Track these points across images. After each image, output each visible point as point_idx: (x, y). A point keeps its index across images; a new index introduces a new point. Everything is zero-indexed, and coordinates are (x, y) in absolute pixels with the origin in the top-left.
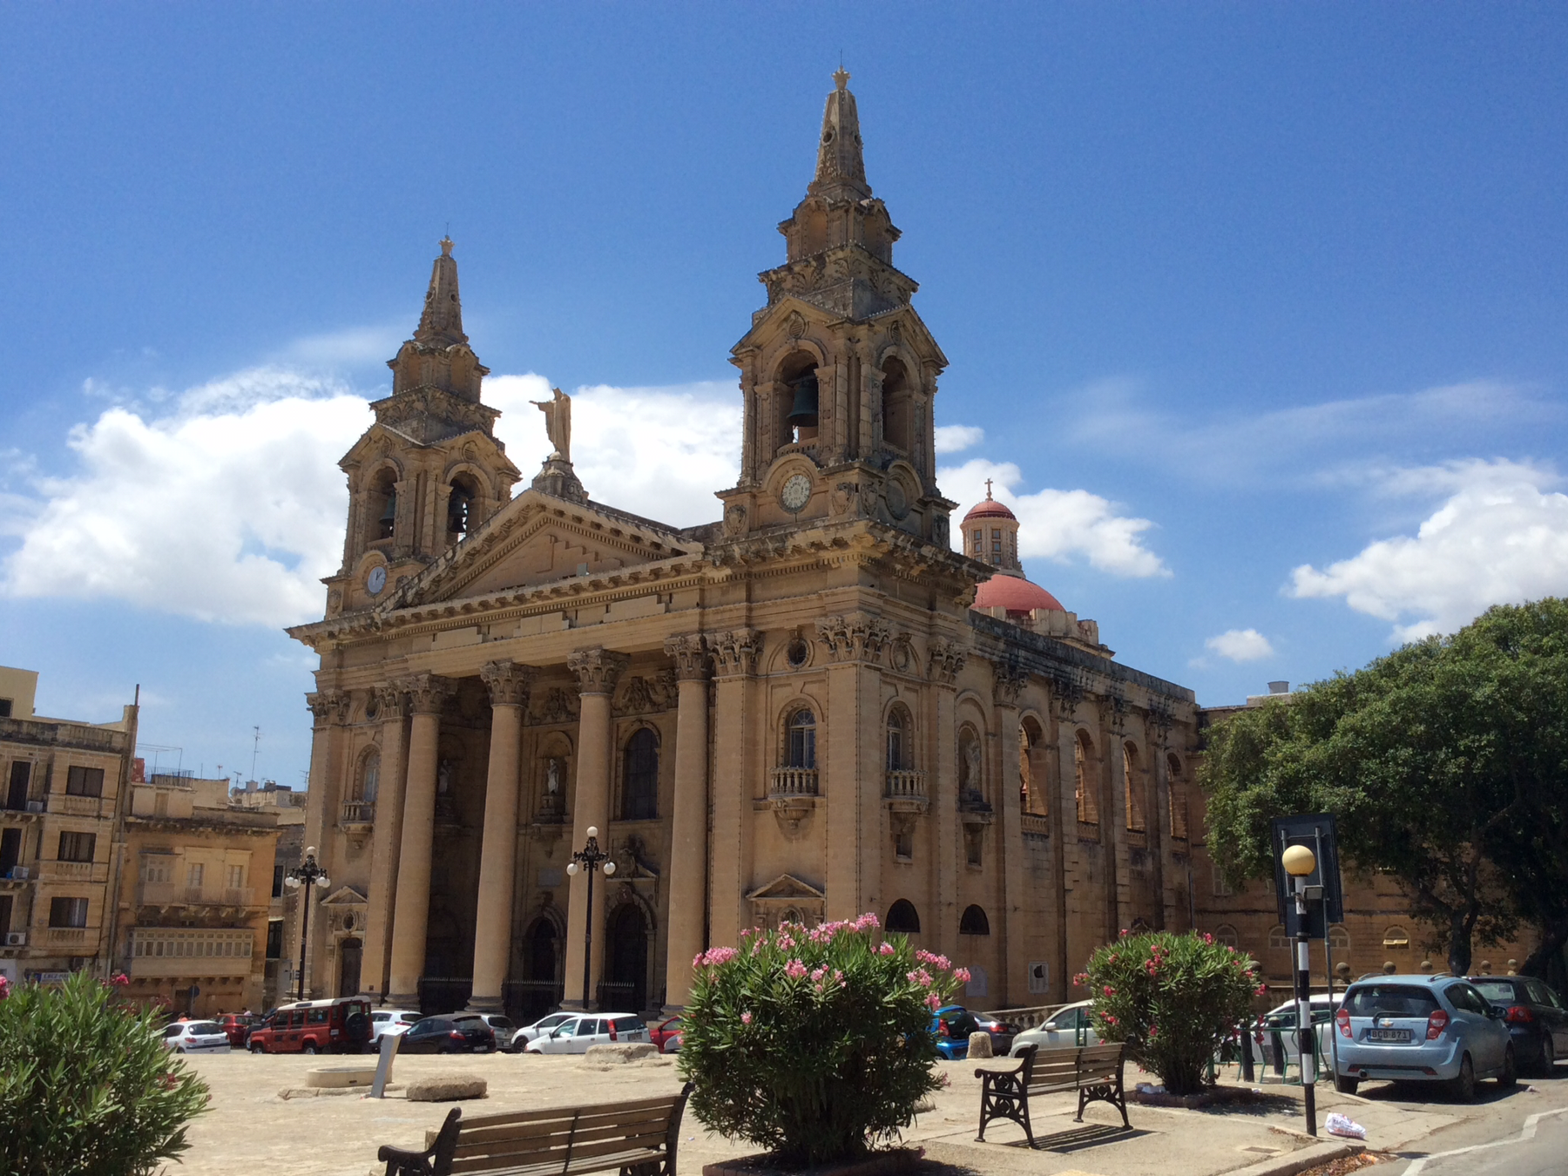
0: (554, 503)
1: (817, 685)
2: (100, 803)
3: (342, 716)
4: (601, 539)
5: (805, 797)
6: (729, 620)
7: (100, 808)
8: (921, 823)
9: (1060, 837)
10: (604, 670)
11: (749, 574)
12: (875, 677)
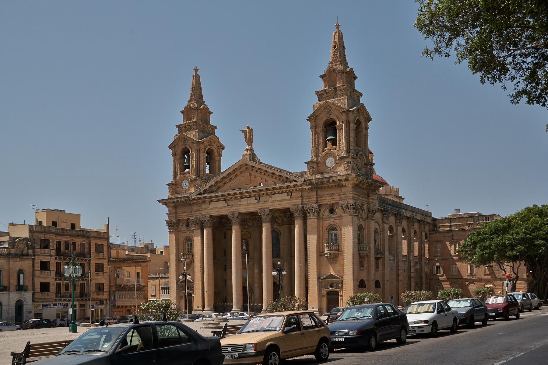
0: (251, 163)
1: (338, 220)
3: (178, 227)
4: (268, 176)
5: (337, 252)
6: (311, 202)
8: (366, 258)
9: (398, 260)
11: (317, 187)
12: (356, 218)
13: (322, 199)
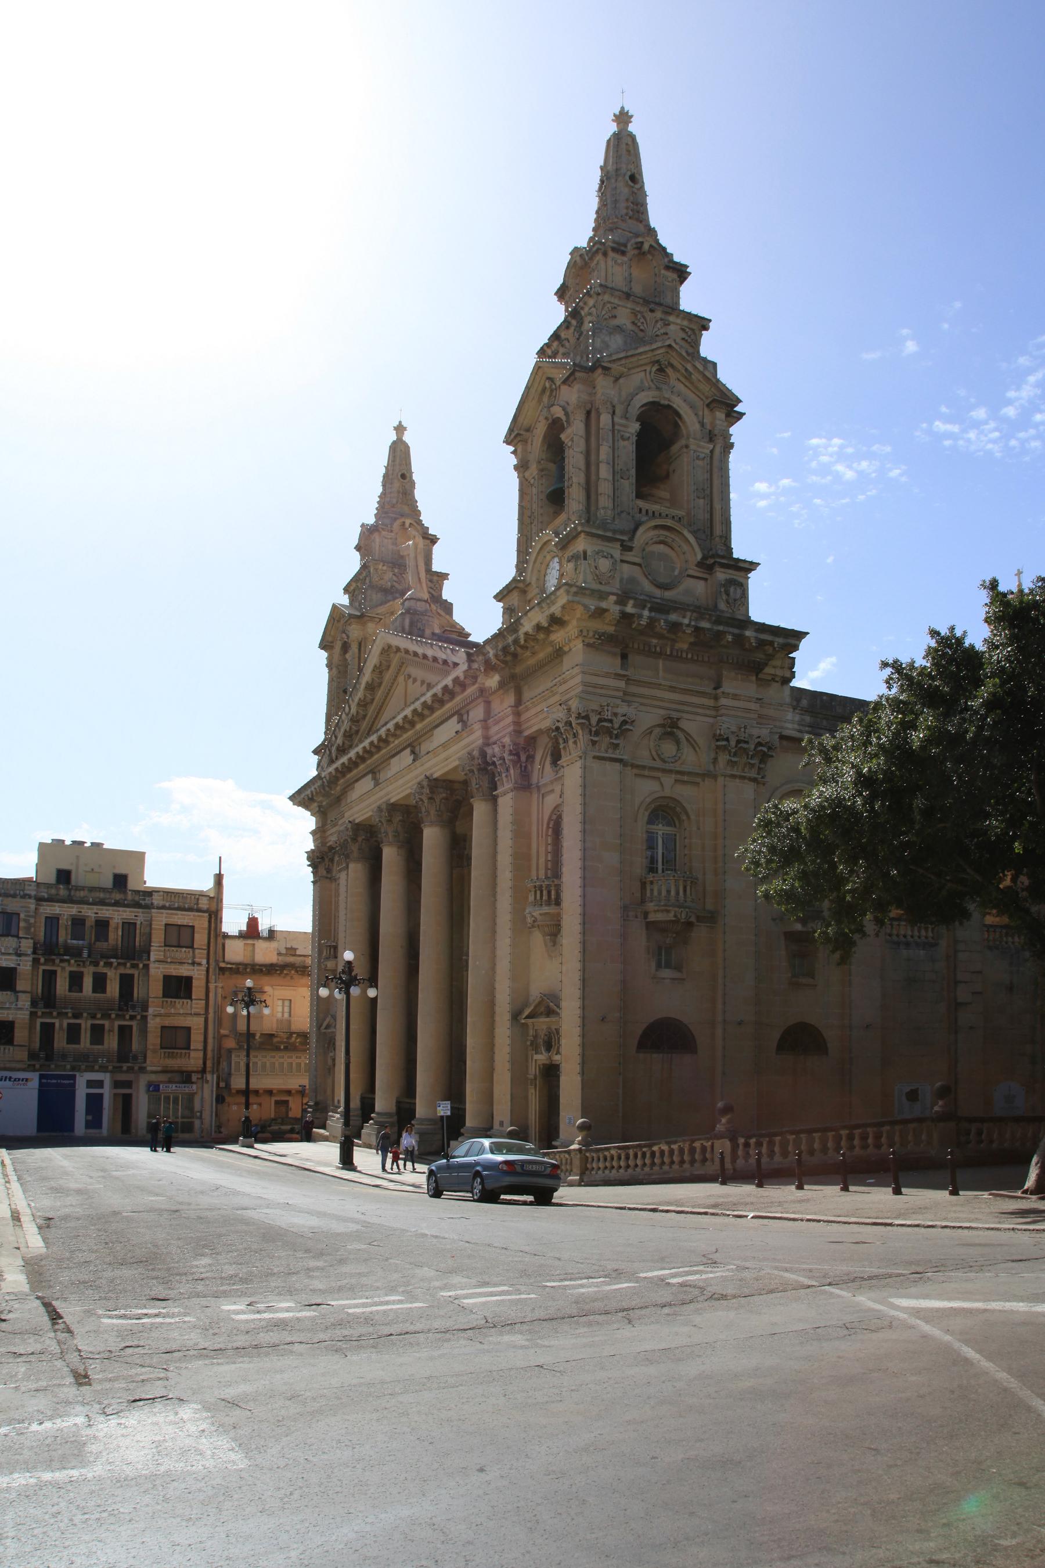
2: (193, 952)
7: (194, 957)
10: (438, 801)
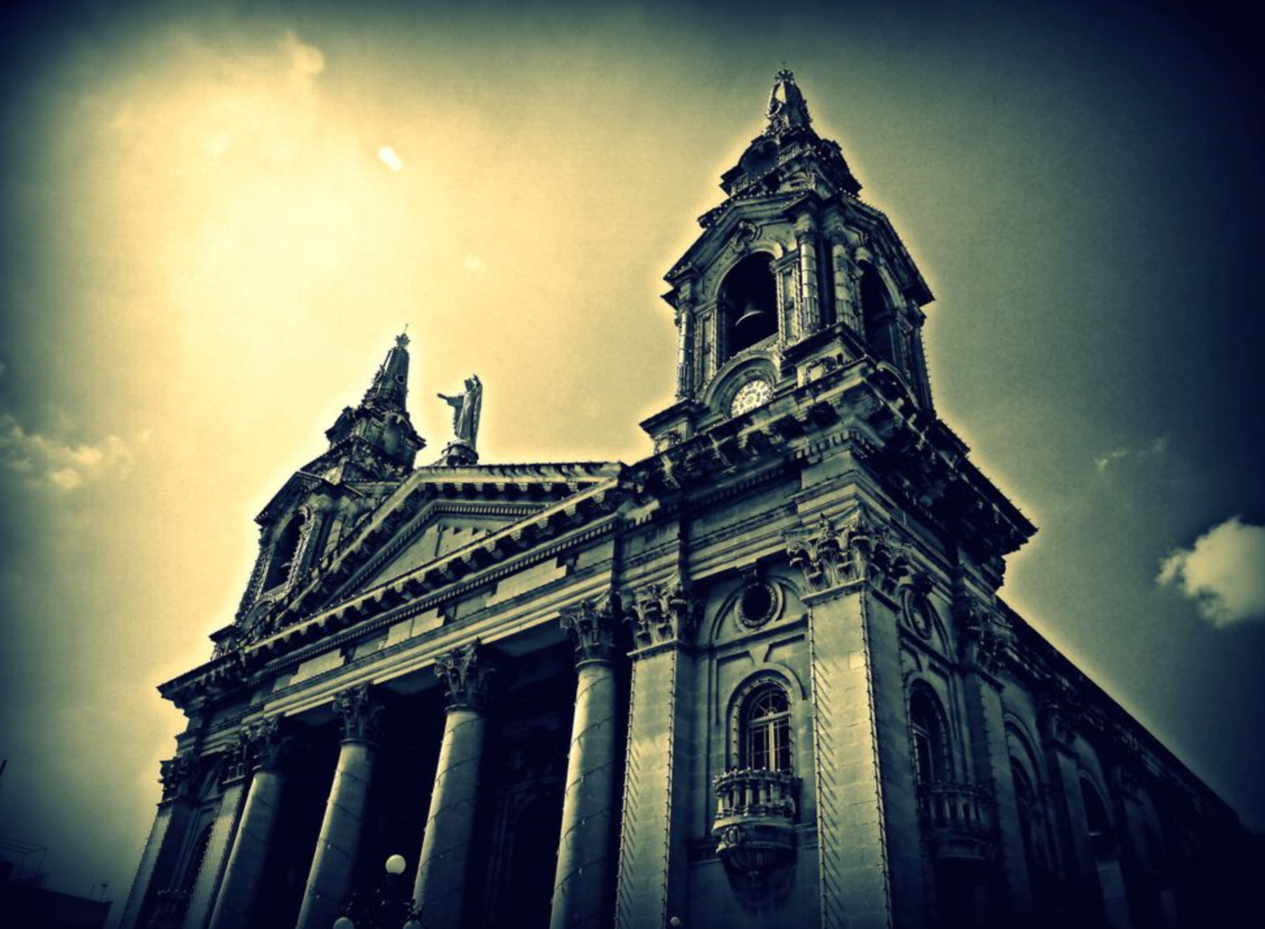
13: (708, 552)
